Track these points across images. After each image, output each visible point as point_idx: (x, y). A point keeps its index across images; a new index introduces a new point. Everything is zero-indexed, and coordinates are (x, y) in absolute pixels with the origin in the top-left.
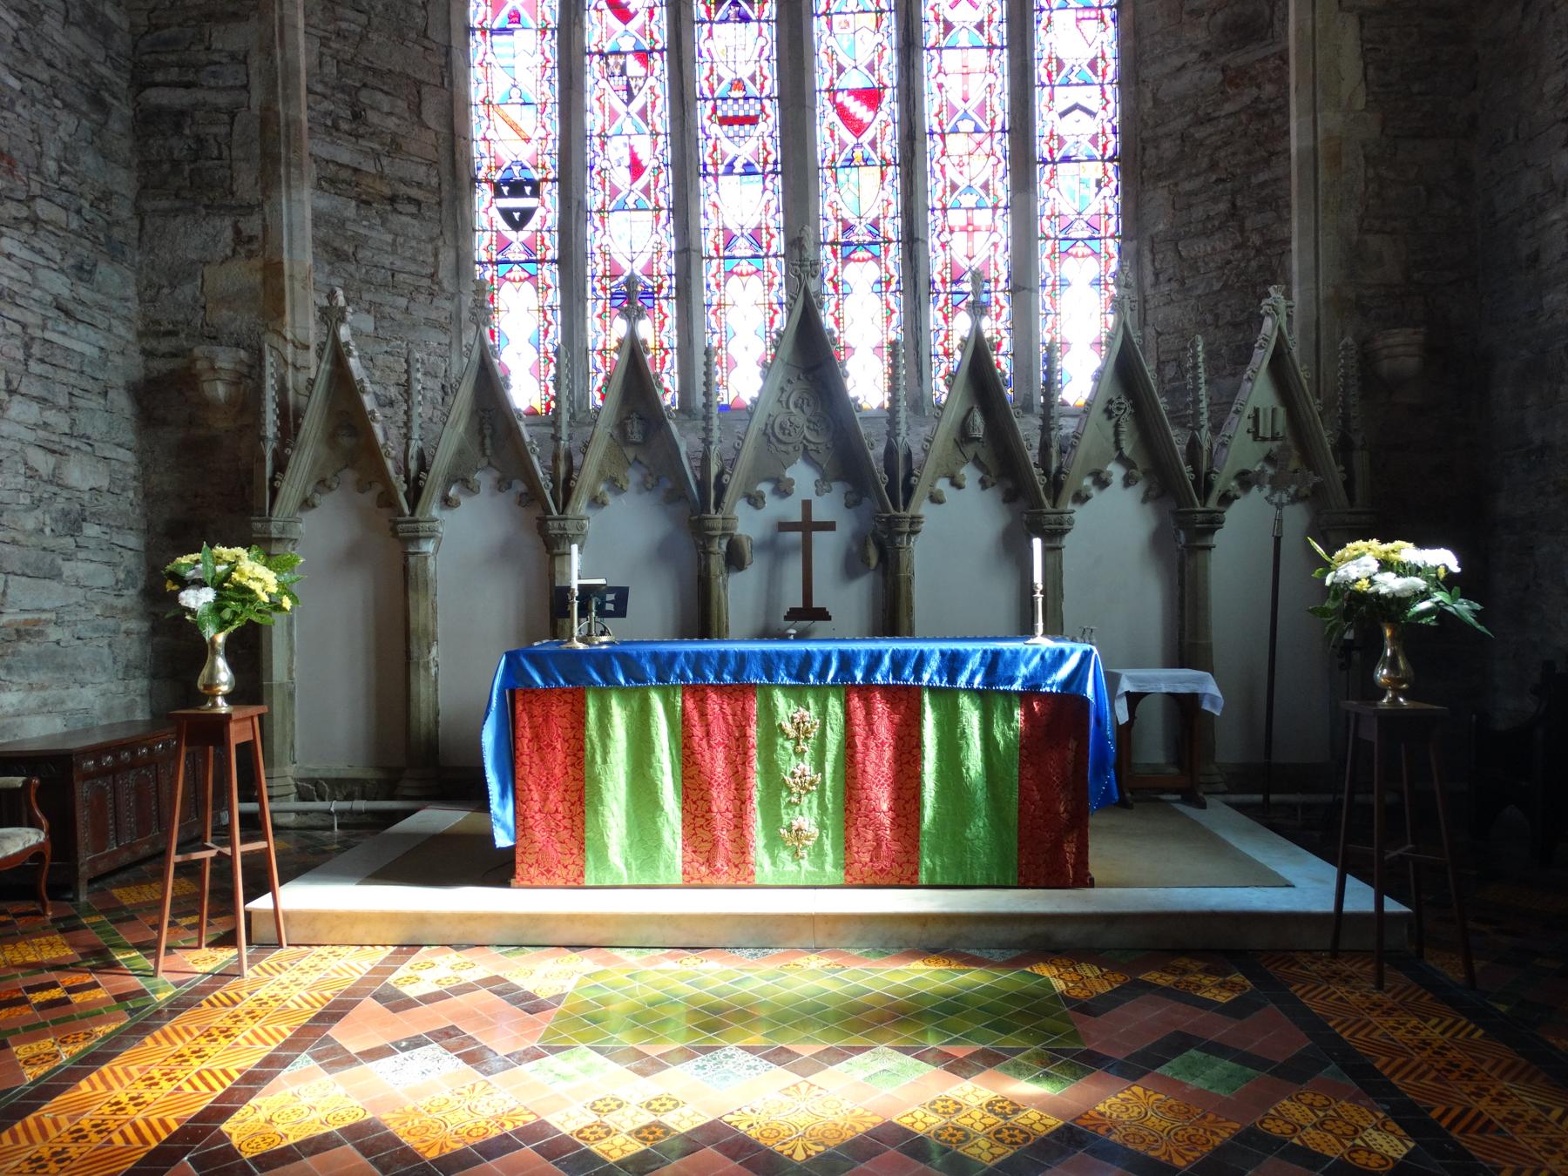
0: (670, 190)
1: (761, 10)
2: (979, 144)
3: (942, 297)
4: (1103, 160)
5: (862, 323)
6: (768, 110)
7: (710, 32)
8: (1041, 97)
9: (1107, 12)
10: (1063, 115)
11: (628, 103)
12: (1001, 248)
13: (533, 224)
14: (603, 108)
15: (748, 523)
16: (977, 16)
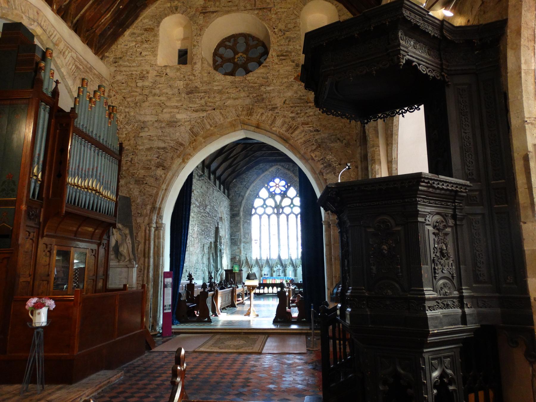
15: (275, 269)
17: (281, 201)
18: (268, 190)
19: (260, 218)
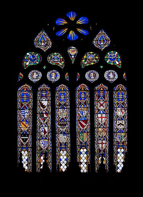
0: (51, 136)
1: (67, 107)
2: (104, 130)
3: (97, 155)
4: (125, 133)
5: (83, 158)
6: (68, 123)
7: (58, 110)
8: (114, 122)
9: (126, 108)
10: (118, 125)
11: (44, 122)
12: (107, 147)
13: (27, 141)
14: (39, 122)
16: (104, 108)
17: (79, 57)
18: (52, 35)
19: (35, 92)
